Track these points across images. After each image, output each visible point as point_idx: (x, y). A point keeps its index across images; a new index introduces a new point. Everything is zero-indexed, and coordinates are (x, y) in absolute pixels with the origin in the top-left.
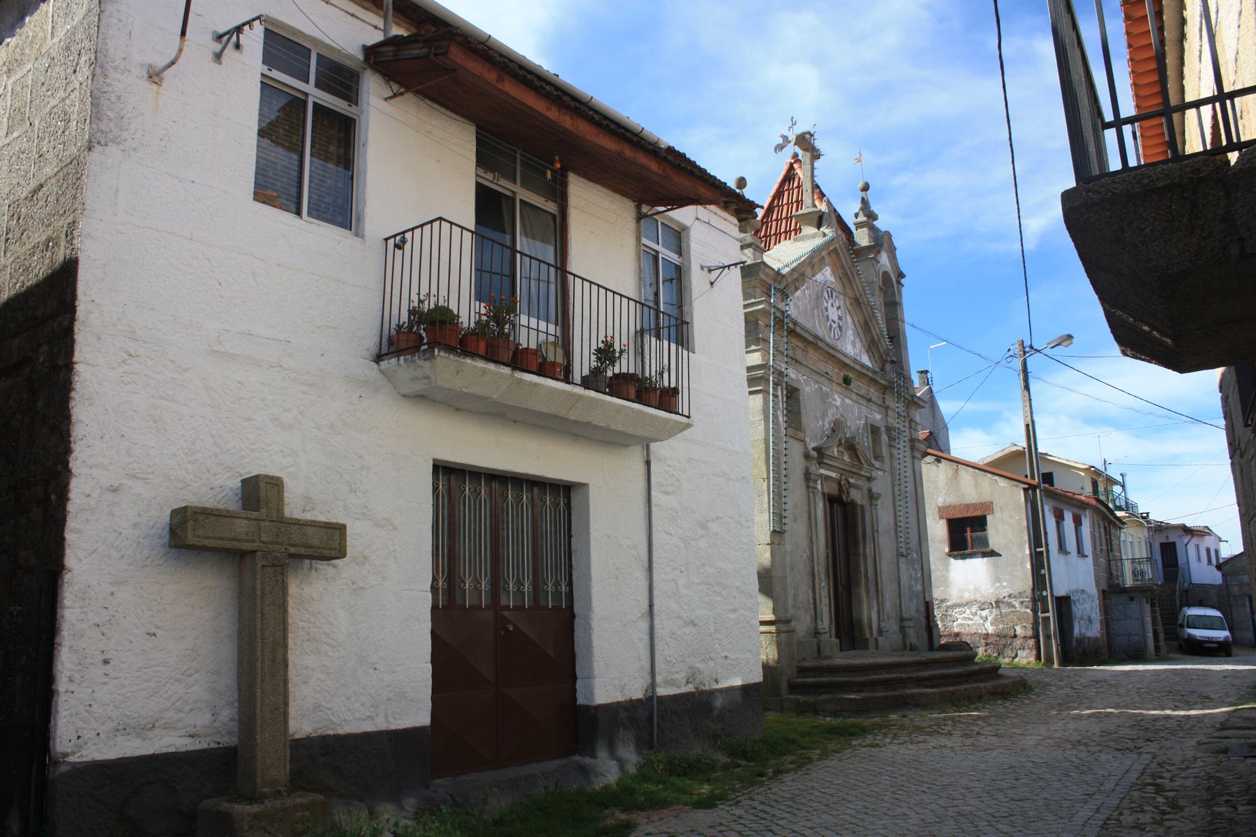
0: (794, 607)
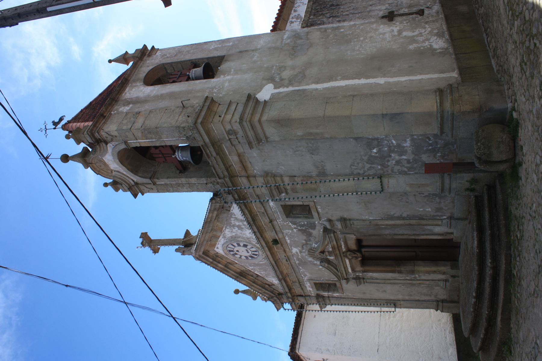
0: (430, 296)
